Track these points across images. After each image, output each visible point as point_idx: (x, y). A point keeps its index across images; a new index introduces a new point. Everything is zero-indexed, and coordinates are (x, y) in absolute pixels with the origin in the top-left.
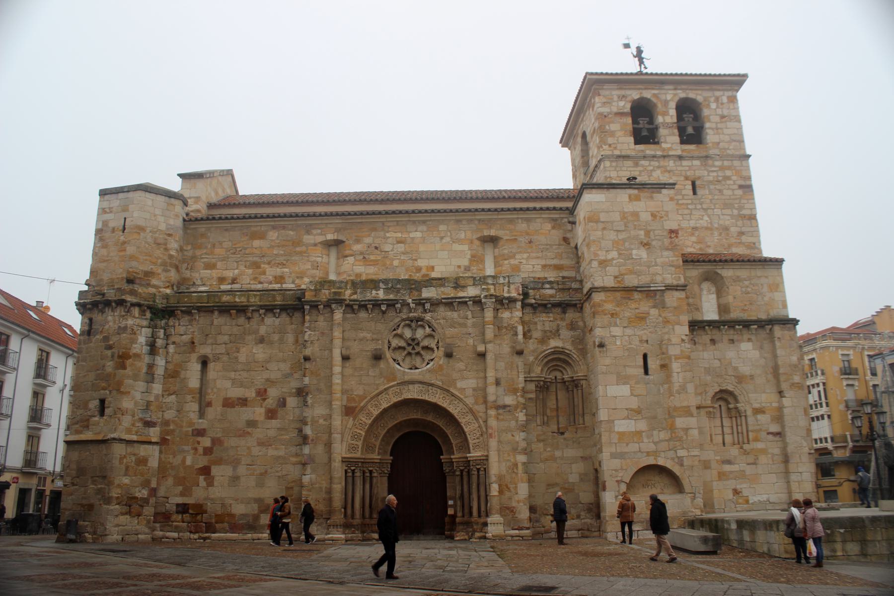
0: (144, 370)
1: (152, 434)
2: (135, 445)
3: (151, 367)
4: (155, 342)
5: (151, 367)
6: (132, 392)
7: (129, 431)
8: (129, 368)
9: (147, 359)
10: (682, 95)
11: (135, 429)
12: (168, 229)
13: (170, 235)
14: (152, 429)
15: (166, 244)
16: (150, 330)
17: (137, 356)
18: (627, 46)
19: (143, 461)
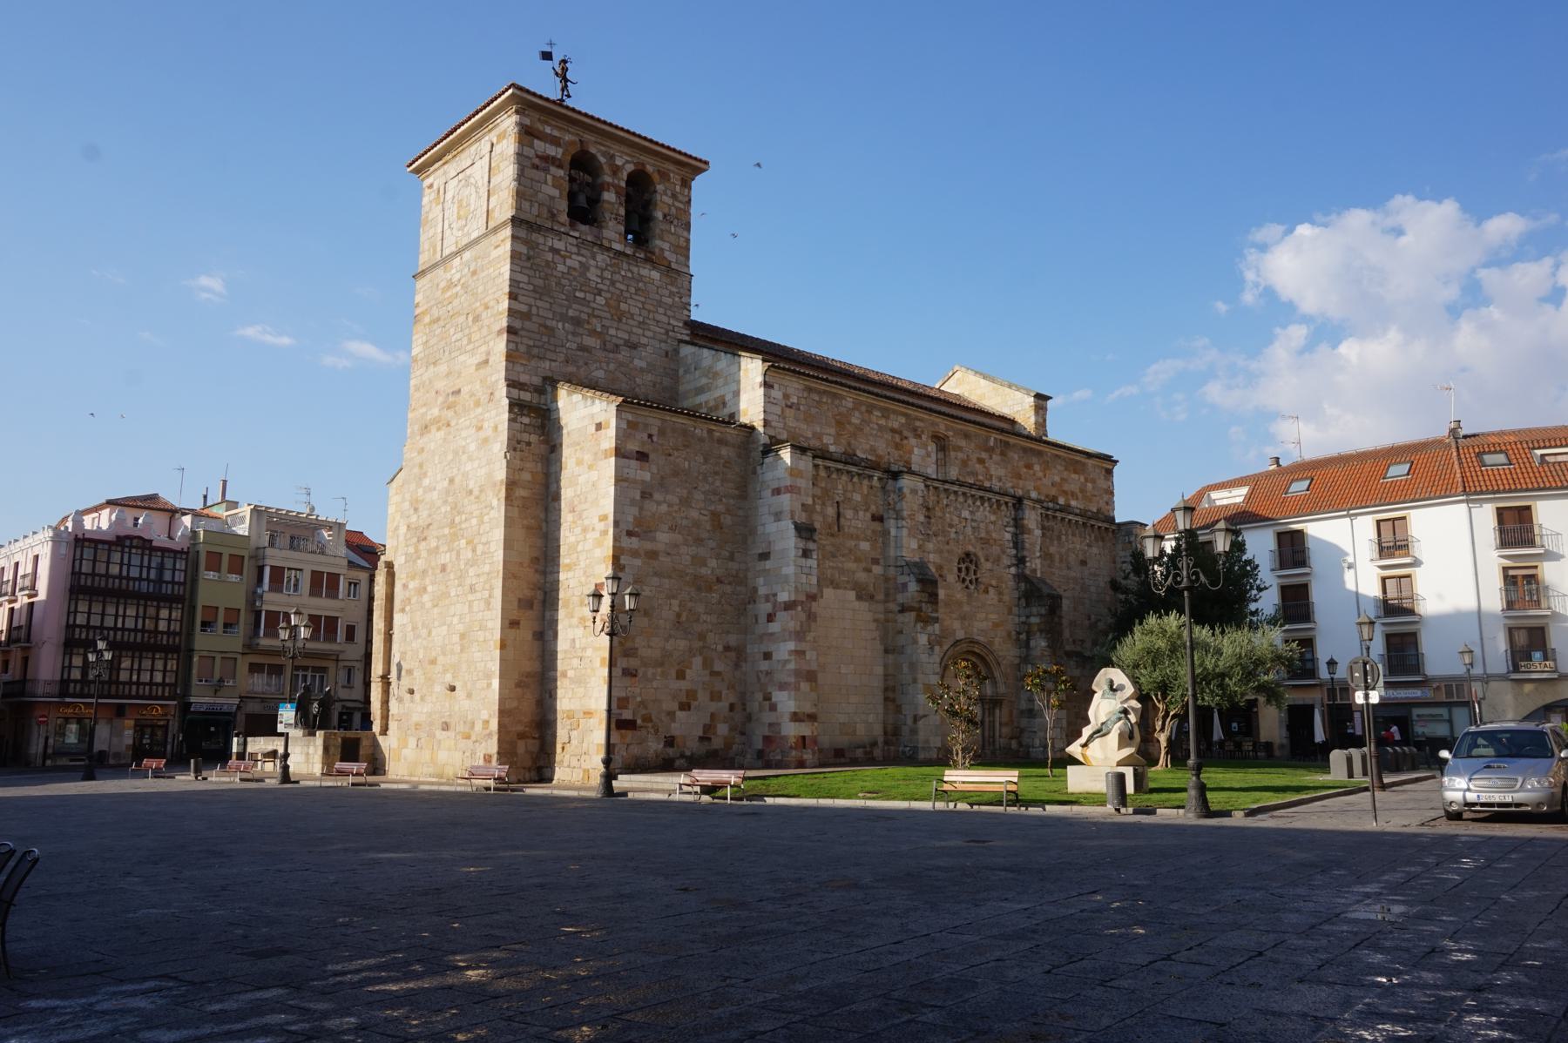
18: (547, 56)
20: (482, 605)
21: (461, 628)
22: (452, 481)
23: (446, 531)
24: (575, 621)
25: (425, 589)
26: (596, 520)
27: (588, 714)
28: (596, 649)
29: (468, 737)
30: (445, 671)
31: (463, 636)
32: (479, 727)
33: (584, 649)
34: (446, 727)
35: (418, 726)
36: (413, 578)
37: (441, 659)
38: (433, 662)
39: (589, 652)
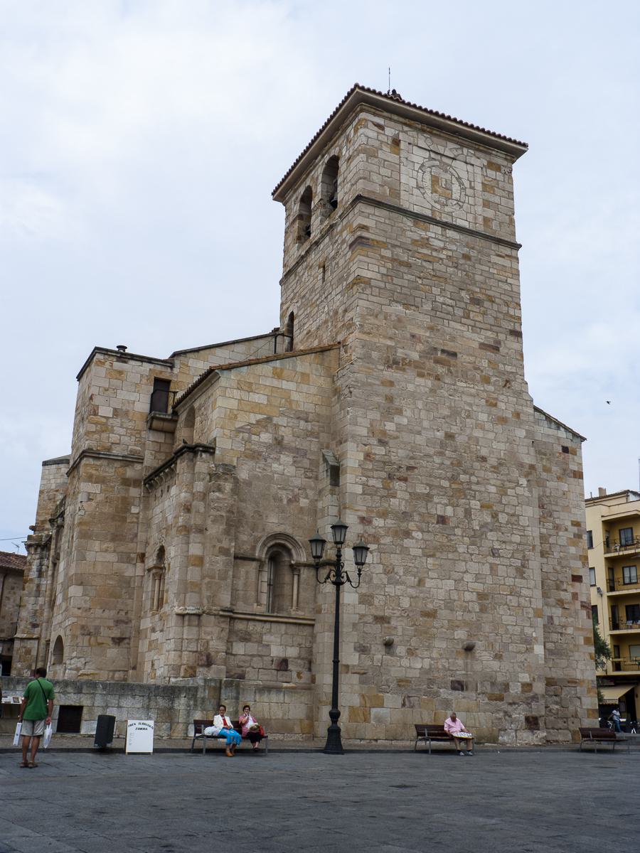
0: (35, 588)
1: (36, 633)
2: (26, 641)
3: (38, 586)
4: (41, 568)
5: (38, 586)
6: (27, 605)
7: (23, 633)
8: (26, 589)
9: (36, 581)
10: (327, 158)
11: (27, 630)
12: (56, 487)
13: (57, 491)
14: (36, 629)
15: (54, 498)
16: (39, 561)
17: (31, 580)
19: (28, 652)
20: (512, 572)
21: (479, 587)
22: (450, 436)
23: (446, 484)
24: (552, 601)
25: (407, 534)
26: (570, 523)
27: (574, 682)
28: (577, 629)
29: (501, 699)
30: (453, 626)
31: (482, 596)
32: (515, 689)
33: (564, 627)
34: (459, 686)
35: (402, 683)
36: (384, 515)
37: (444, 613)
38: (431, 615)
39: (570, 630)
